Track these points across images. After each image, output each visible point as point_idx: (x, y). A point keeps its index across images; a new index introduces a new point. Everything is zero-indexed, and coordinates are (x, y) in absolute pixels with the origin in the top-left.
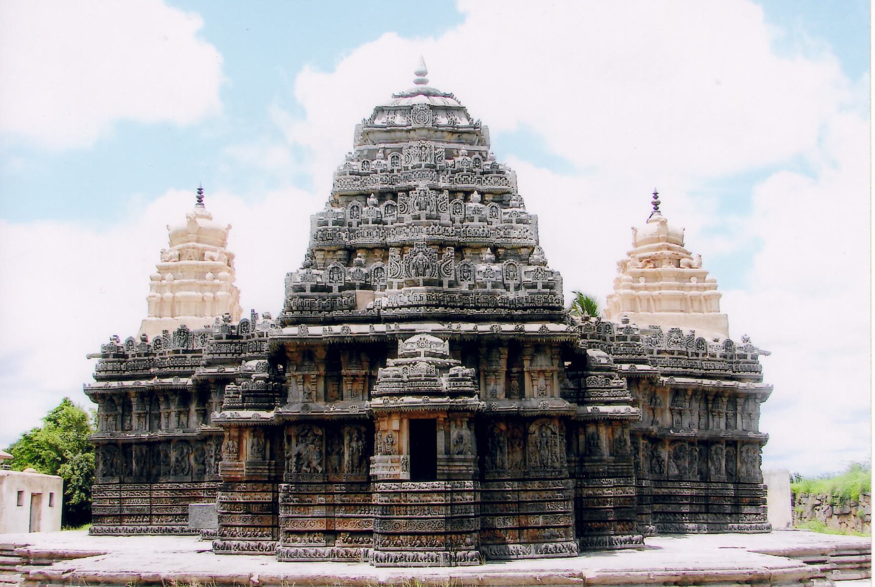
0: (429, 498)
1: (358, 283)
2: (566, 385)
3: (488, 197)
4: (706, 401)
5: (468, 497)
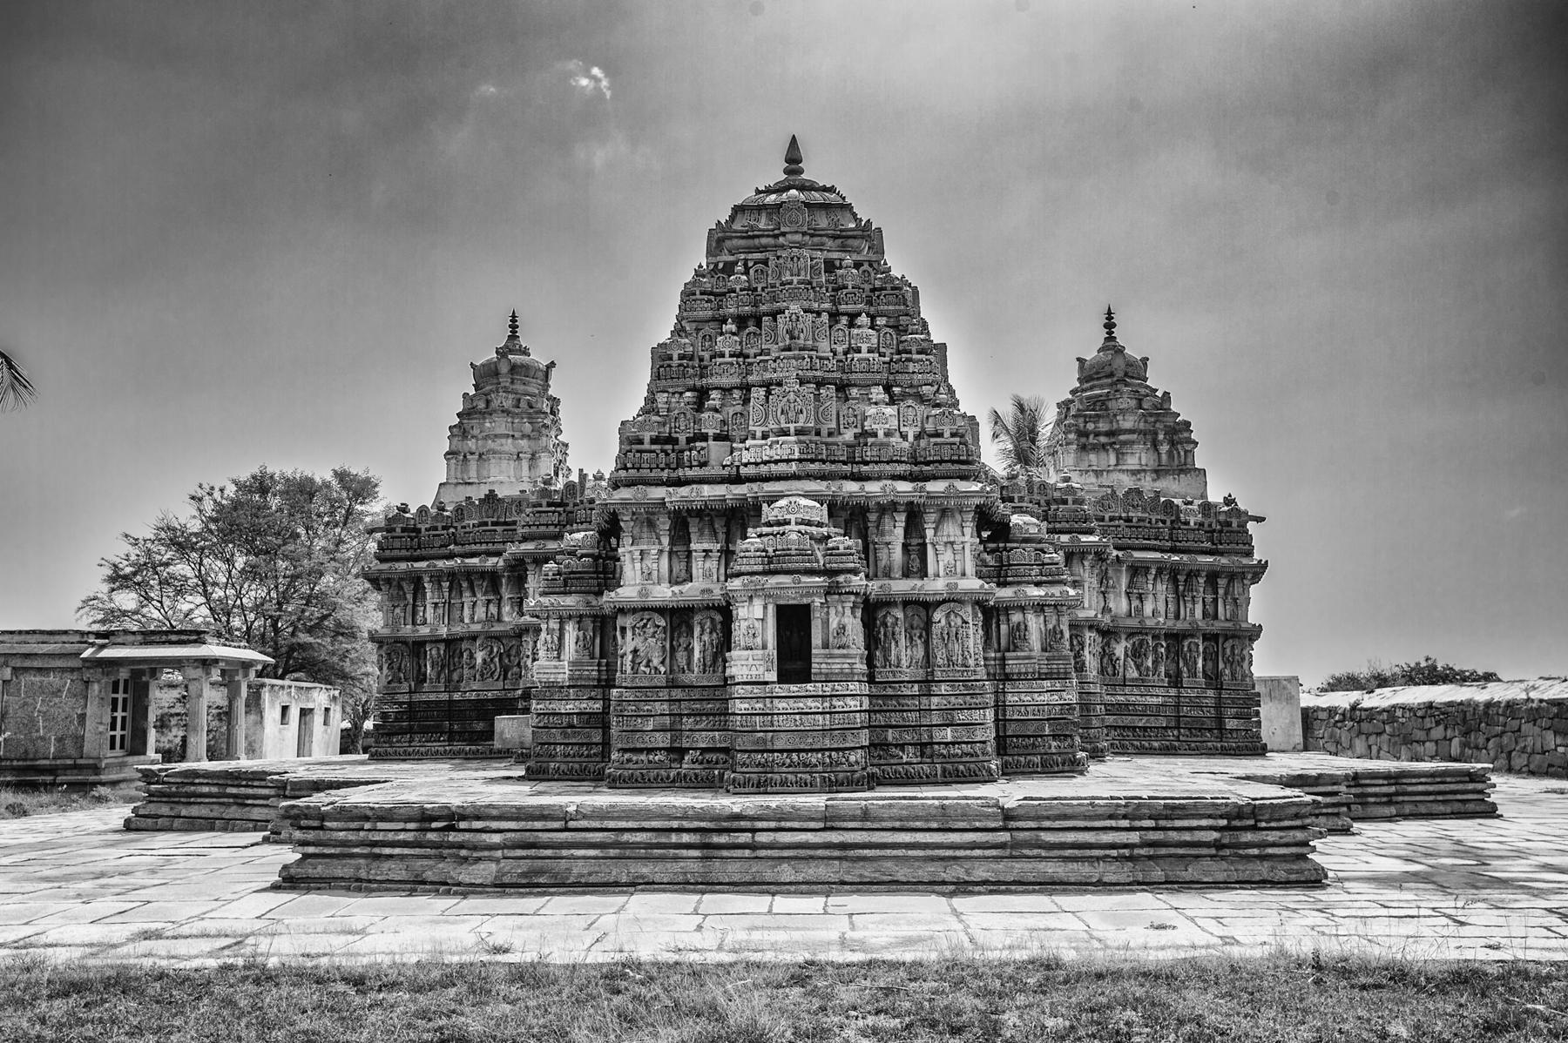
1: (711, 432)
2: (983, 561)
3: (881, 321)
4: (1175, 581)
5: (853, 704)
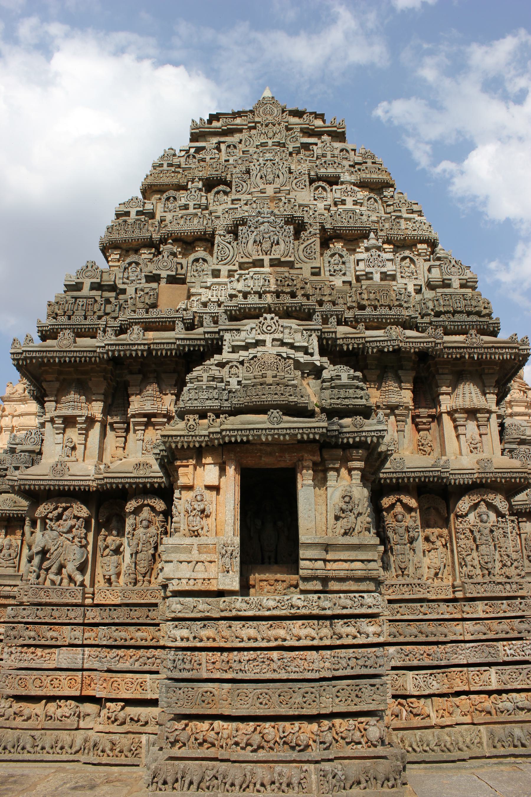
0: (282, 633)
1: (164, 274)
